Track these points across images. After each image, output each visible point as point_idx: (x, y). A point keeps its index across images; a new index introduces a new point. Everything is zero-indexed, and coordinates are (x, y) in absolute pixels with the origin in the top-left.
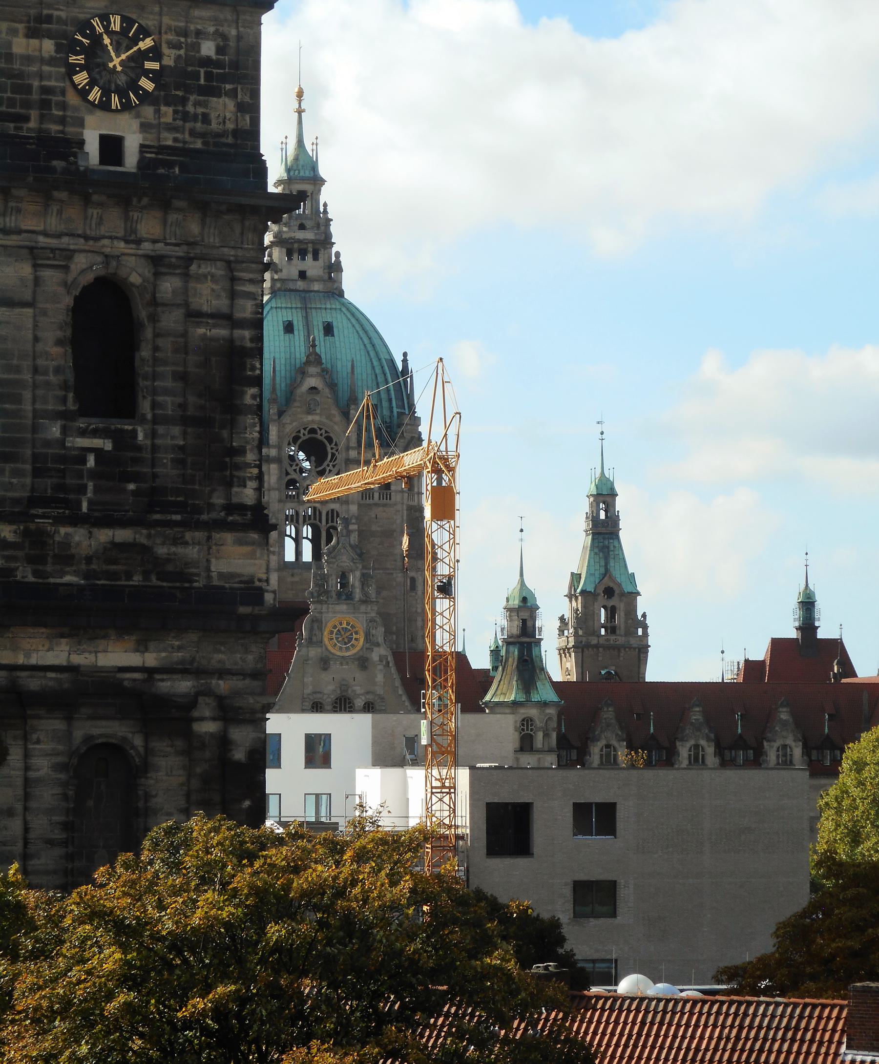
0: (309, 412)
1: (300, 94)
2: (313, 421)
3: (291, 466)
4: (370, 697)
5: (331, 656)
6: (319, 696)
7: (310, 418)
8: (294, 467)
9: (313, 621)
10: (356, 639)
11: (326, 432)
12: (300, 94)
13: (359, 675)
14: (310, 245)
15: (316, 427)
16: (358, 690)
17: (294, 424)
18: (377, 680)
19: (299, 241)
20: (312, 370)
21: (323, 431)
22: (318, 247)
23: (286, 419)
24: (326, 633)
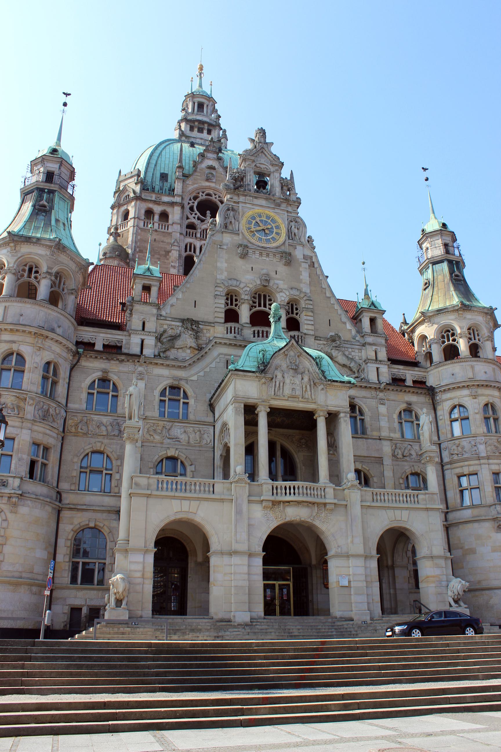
0: (208, 180)
1: (201, 68)
2: (210, 188)
3: (191, 214)
4: (295, 292)
5: (249, 245)
6: (234, 283)
7: (207, 184)
8: (193, 215)
9: (228, 210)
10: (277, 234)
11: (219, 197)
12: (201, 68)
13: (282, 269)
14: (206, 125)
15: (211, 192)
16: (282, 284)
17: (195, 186)
18: (301, 277)
19: (200, 122)
20: (210, 155)
21: (217, 196)
22: (211, 128)
23: (189, 182)
24: (243, 221)
